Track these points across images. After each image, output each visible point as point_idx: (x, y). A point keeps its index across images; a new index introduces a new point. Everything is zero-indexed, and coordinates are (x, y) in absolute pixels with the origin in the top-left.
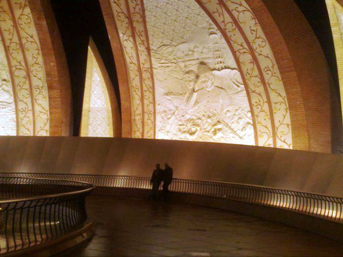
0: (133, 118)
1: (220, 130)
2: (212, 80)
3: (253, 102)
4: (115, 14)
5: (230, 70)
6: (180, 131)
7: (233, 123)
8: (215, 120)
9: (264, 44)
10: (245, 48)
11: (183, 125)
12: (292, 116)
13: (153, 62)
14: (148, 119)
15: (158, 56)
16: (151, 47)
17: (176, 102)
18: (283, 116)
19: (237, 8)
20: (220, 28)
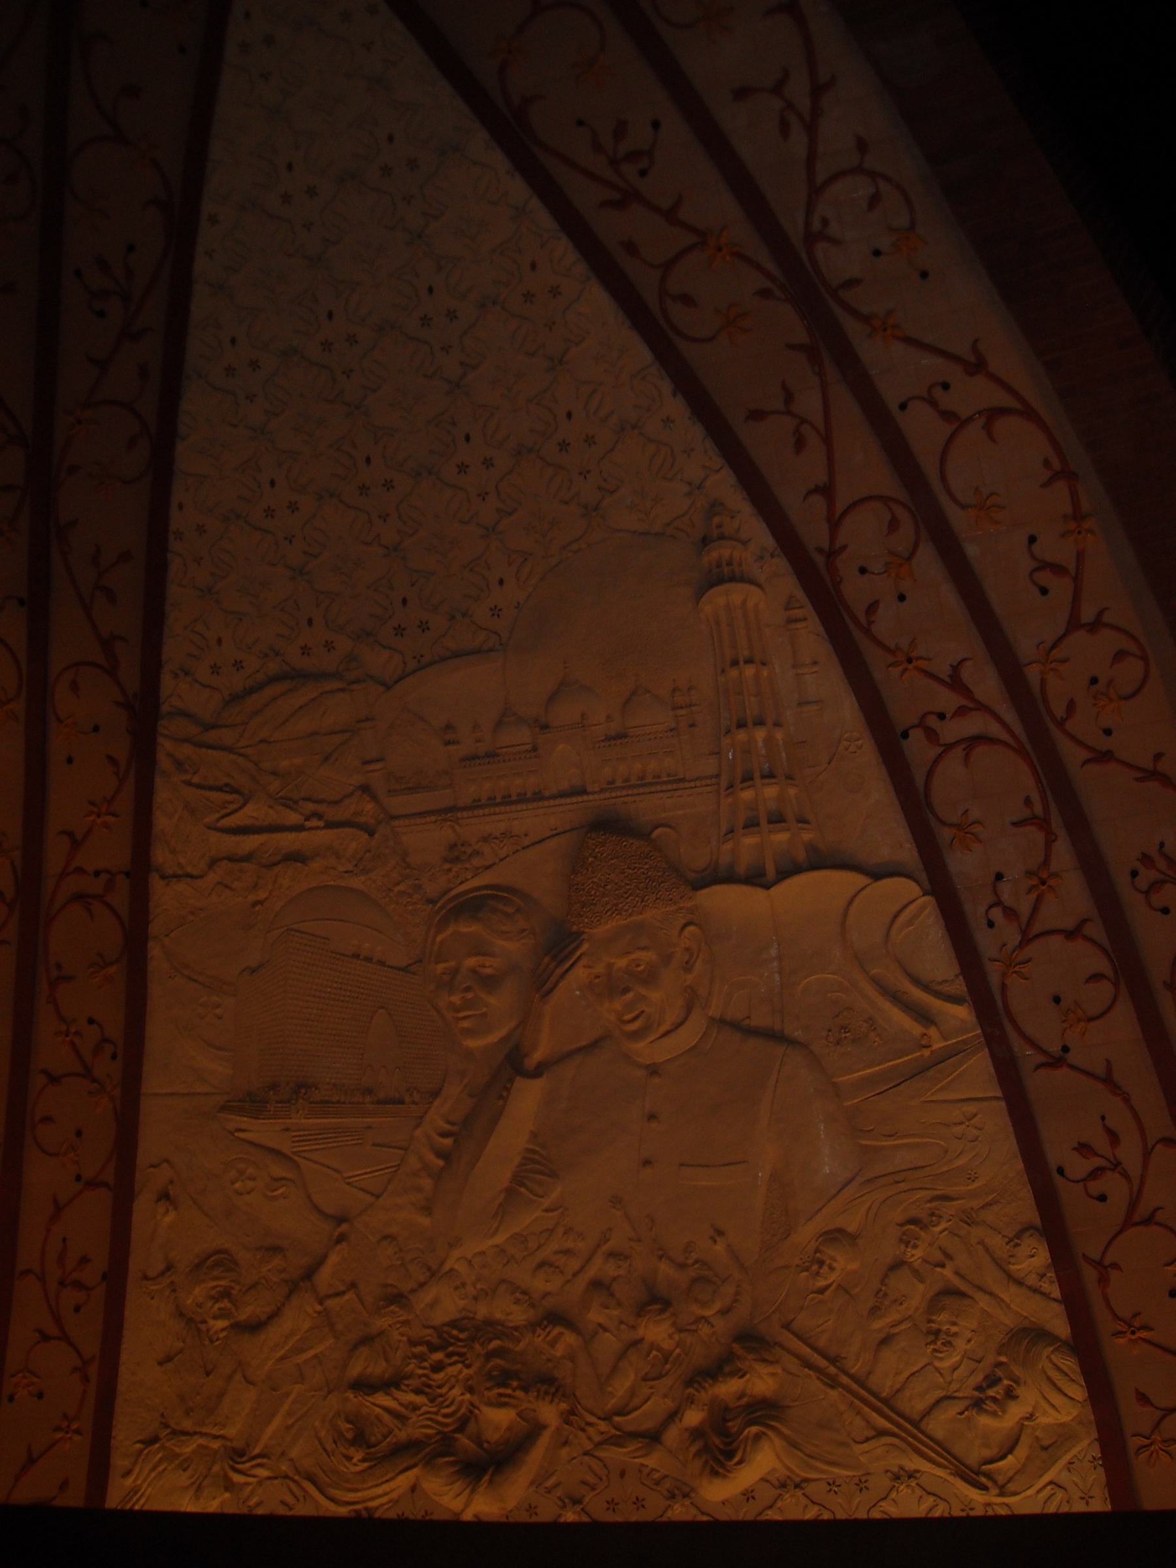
1: (764, 1411)
2: (688, 967)
5: (861, 880)
6: (360, 1439)
7: (886, 1340)
10: (982, 707)
11: (389, 1384)
13: (162, 822)
14: (45, 1338)
16: (174, 691)
19: (946, 386)
20: (788, 541)
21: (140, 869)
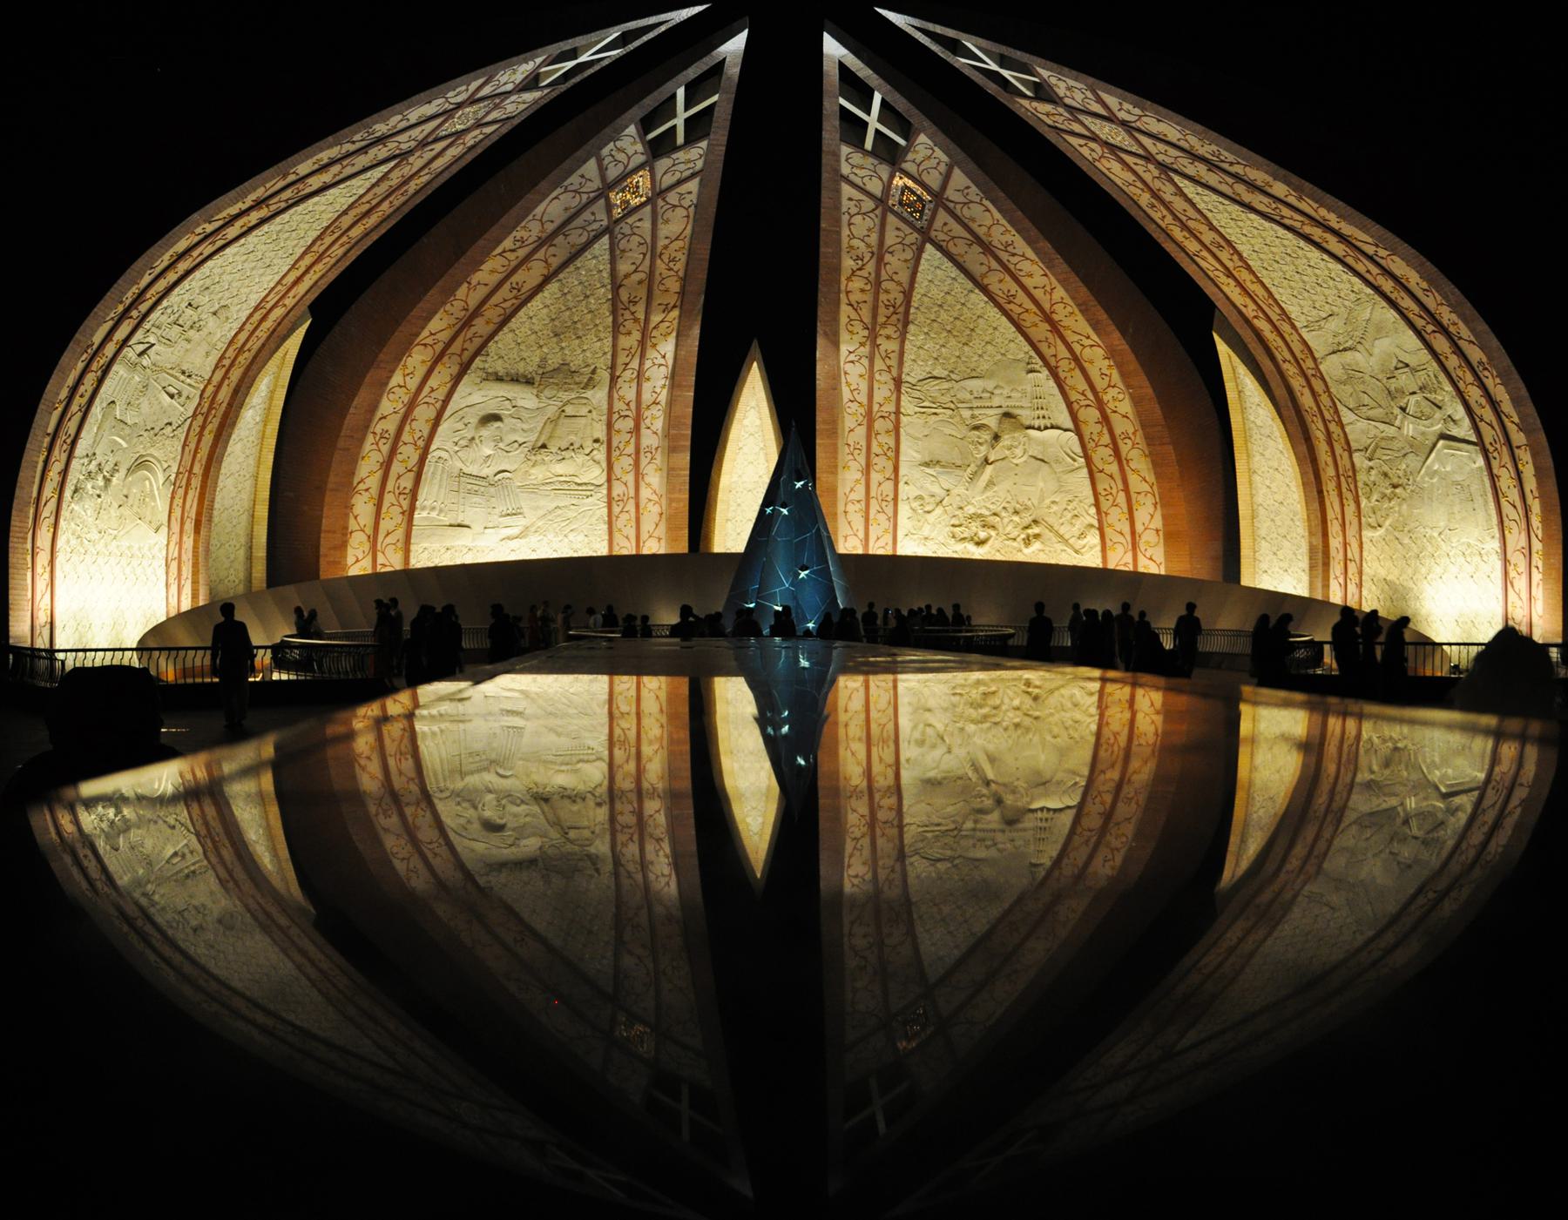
0: (841, 508)
1: (1037, 536)
3: (1100, 488)
4: (843, 320)
8: (1028, 520)
9: (1121, 396)
12: (1164, 517)
15: (917, 394)
17: (947, 481)
18: (1149, 516)
20: (1046, 364)
21: (898, 412)
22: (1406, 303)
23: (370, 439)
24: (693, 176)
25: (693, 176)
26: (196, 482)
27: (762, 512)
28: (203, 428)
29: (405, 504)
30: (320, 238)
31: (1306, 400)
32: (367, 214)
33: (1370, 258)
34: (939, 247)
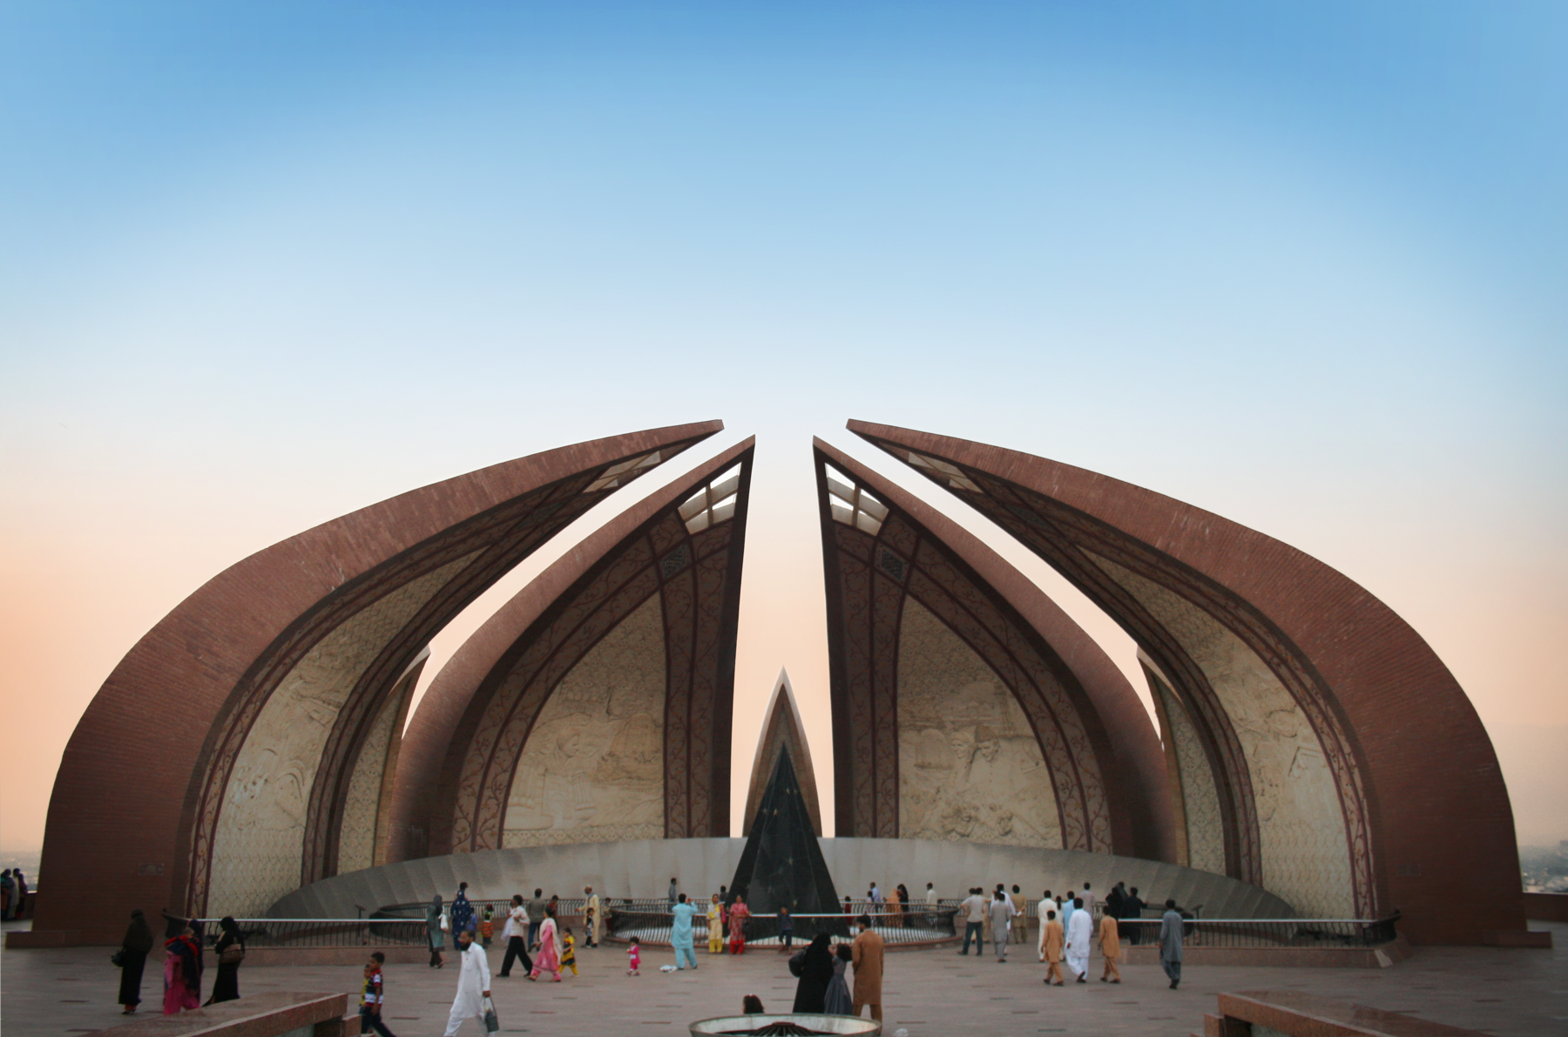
21: (895, 721)
22: (1255, 640)
23: (474, 745)
24: (722, 548)
25: (722, 548)
26: (332, 781)
27: (760, 813)
28: (339, 739)
29: (501, 797)
30: (435, 597)
31: (1209, 714)
32: (470, 581)
33: (1224, 608)
34: (916, 597)
